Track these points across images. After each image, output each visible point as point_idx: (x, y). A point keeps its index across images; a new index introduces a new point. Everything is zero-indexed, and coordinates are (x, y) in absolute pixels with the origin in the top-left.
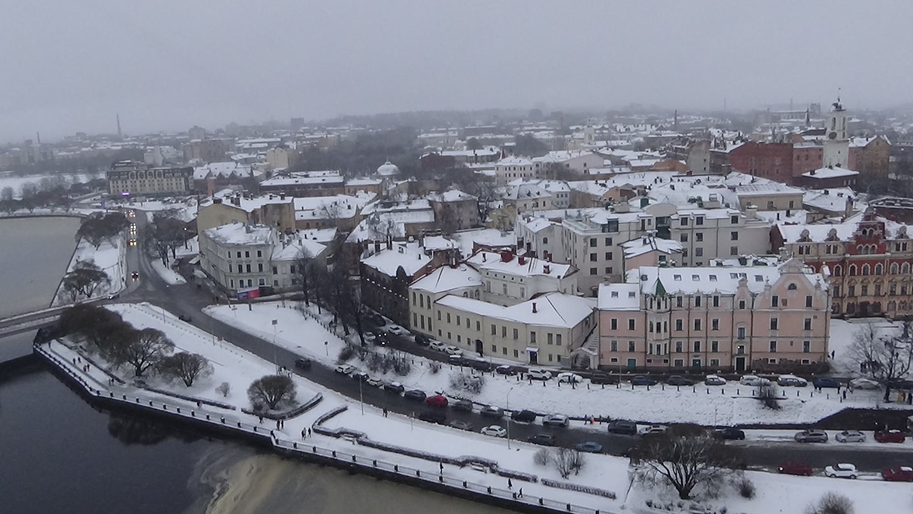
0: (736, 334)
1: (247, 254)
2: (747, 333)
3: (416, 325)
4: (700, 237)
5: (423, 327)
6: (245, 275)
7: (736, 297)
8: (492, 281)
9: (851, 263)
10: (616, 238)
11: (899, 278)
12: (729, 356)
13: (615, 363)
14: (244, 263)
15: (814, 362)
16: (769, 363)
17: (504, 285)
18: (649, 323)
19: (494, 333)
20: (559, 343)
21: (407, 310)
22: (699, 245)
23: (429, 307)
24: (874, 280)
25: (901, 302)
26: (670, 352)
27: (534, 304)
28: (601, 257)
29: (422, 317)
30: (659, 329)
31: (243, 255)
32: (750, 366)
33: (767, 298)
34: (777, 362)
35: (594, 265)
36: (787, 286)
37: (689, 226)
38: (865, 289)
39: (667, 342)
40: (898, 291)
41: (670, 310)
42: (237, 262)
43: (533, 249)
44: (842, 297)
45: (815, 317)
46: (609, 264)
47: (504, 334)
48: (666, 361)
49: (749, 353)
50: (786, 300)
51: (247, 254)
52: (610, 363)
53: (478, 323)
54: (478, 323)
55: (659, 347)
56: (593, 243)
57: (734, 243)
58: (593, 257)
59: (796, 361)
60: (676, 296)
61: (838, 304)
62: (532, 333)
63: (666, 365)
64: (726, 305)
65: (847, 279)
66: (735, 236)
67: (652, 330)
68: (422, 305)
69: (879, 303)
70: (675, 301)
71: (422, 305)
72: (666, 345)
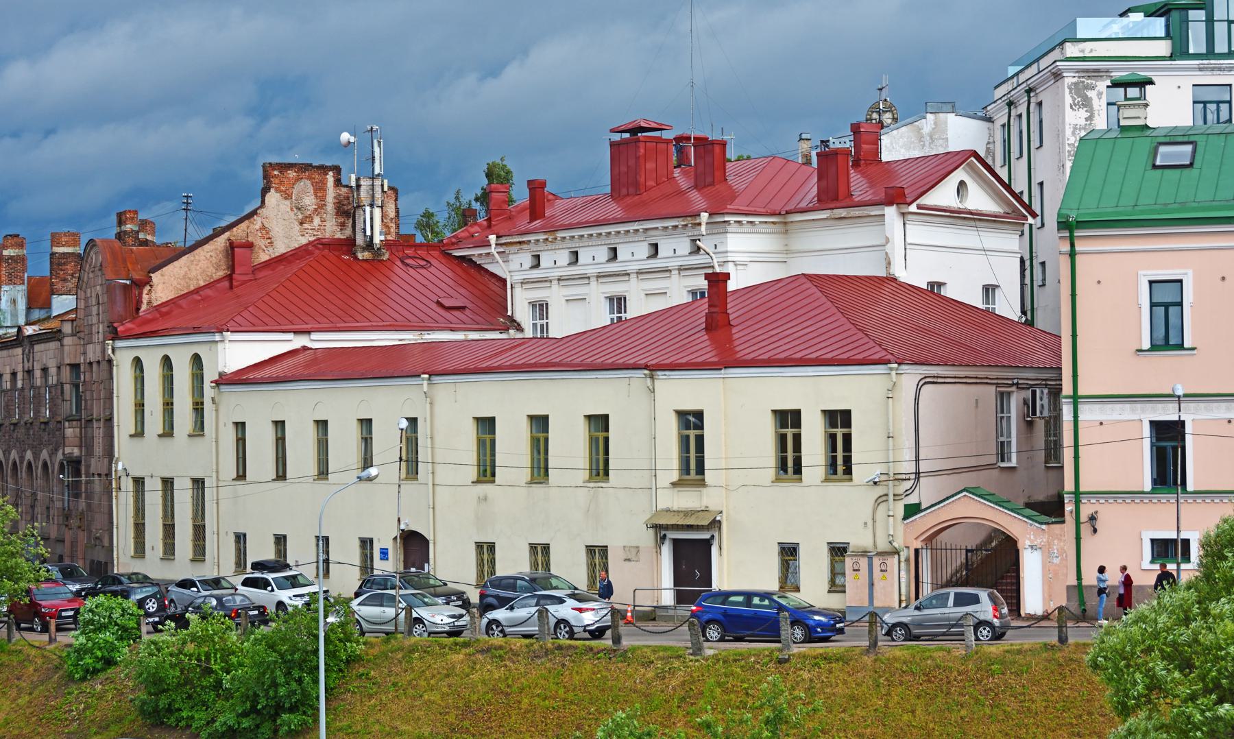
8: (555, 296)
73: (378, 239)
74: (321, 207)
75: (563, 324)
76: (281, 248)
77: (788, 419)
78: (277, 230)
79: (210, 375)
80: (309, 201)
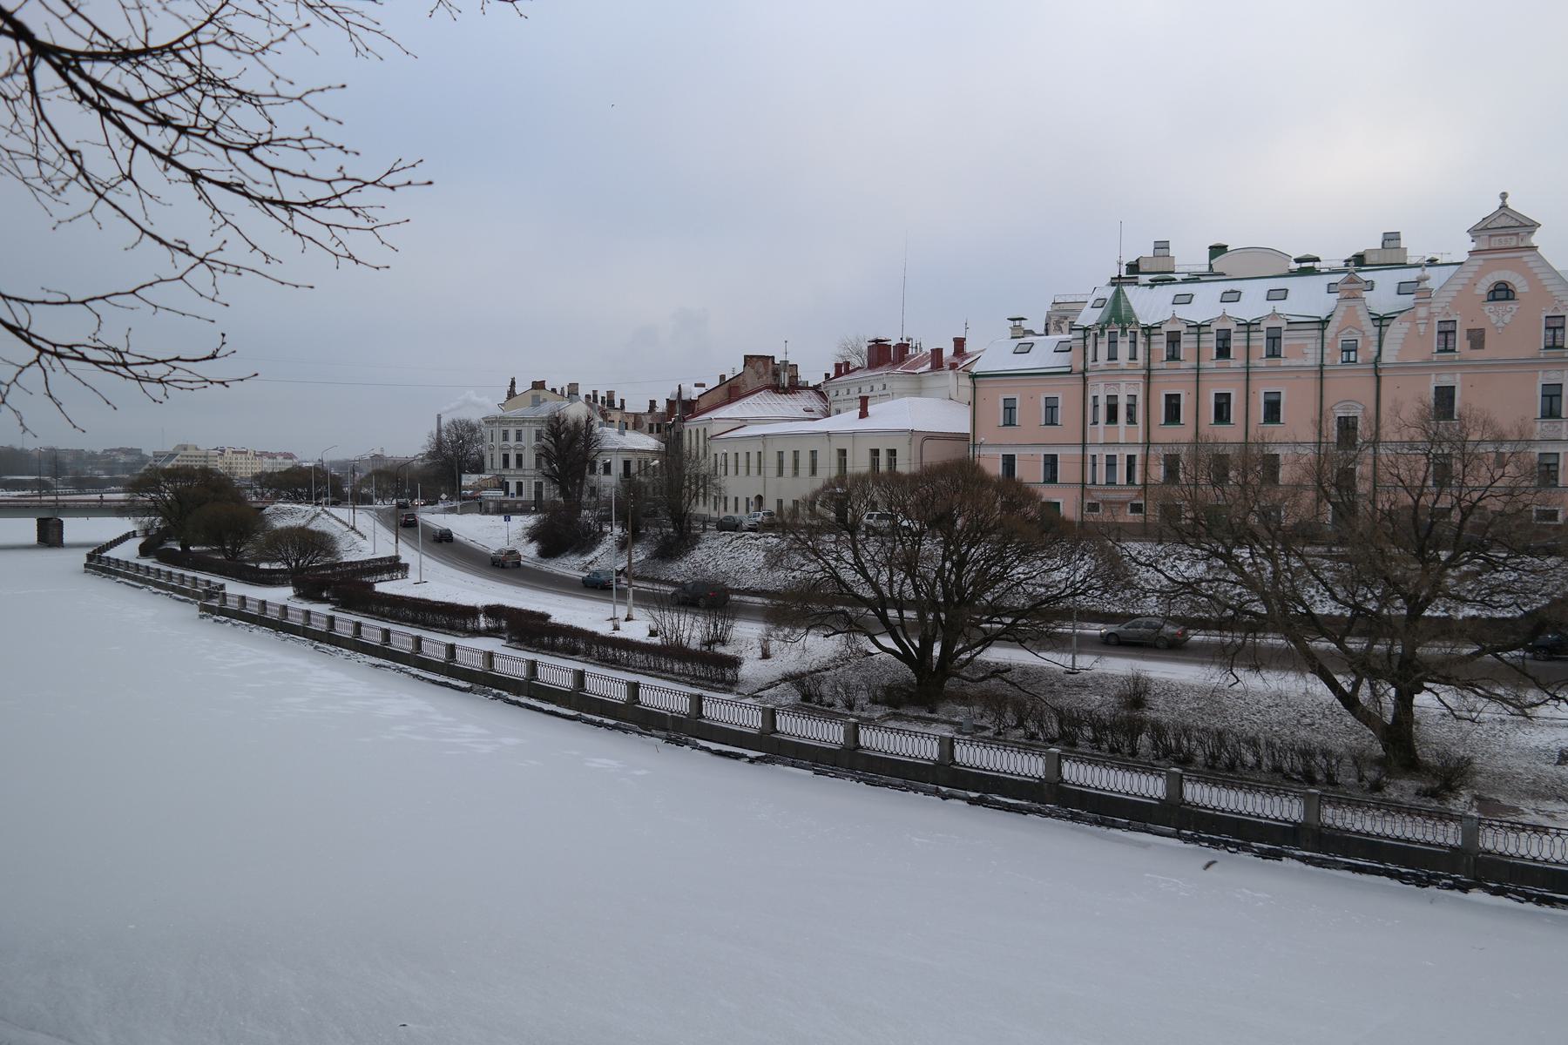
1: (519, 437)
6: (512, 473)
7: (1330, 331)
14: (512, 451)
18: (1090, 401)
30: (1112, 416)
31: (512, 436)
33: (1422, 328)
36: (1483, 287)
39: (1138, 452)
42: (501, 449)
50: (1482, 331)
51: (519, 437)
55: (1111, 462)
60: (1166, 328)
63: (1138, 518)
64: (1302, 351)
67: (1095, 423)
70: (1160, 344)
73: (786, 385)
74: (766, 373)
78: (749, 381)
80: (762, 370)
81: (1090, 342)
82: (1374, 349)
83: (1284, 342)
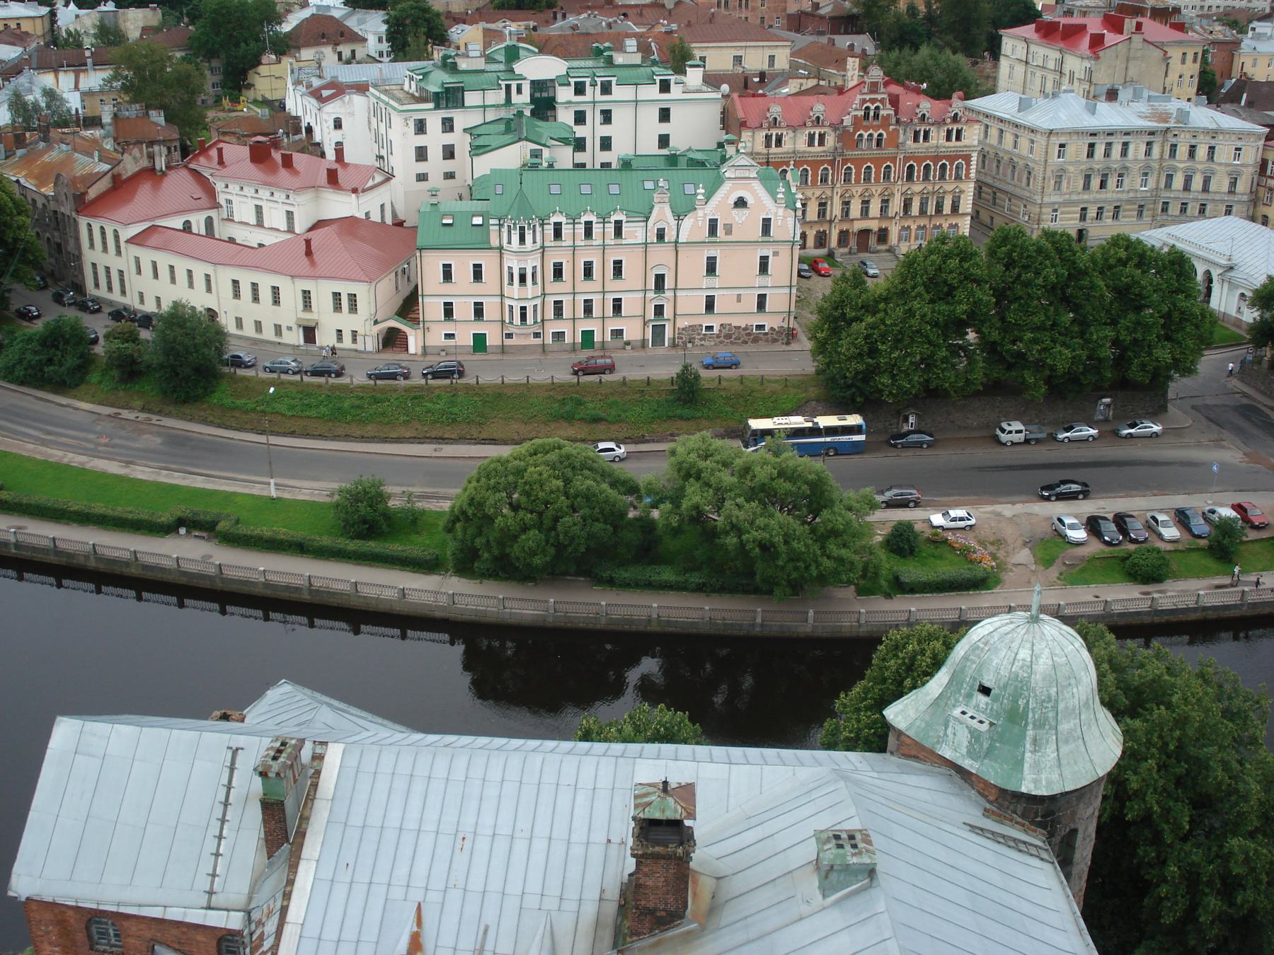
0: (651, 284)
2: (668, 283)
3: (97, 285)
4: (607, 117)
5: (110, 289)
9: (845, 161)
10: (462, 119)
11: (917, 188)
12: (639, 322)
13: (451, 342)
15: (772, 329)
16: (704, 332)
17: (257, 206)
19: (237, 295)
20: (353, 308)
21: (78, 257)
22: (605, 131)
23: (119, 252)
24: (879, 192)
25: (919, 228)
26: (543, 321)
27: (308, 242)
28: (435, 153)
29: (108, 269)
30: (523, 279)
32: (674, 338)
33: (700, 223)
34: (716, 331)
35: (422, 167)
37: (588, 97)
38: (866, 203)
39: (538, 302)
40: (915, 209)
41: (543, 247)
43: (317, 138)
44: (831, 222)
45: (776, 254)
46: (449, 166)
47: (256, 299)
48: (537, 335)
49: (672, 318)
52: (442, 341)
53: (208, 277)
54: (208, 277)
55: (523, 309)
56: (421, 127)
57: (664, 128)
58: (421, 154)
59: (746, 329)
61: (824, 232)
62: (304, 292)
63: (538, 341)
65: (839, 189)
66: (665, 115)
68: (105, 249)
69: (886, 230)
71: (105, 249)
72: (535, 306)
75: (252, 237)
76: (130, 174)
77: (337, 296)
79: (123, 239)
80: (138, 155)
81: (505, 230)
82: (675, 233)
83: (624, 230)
